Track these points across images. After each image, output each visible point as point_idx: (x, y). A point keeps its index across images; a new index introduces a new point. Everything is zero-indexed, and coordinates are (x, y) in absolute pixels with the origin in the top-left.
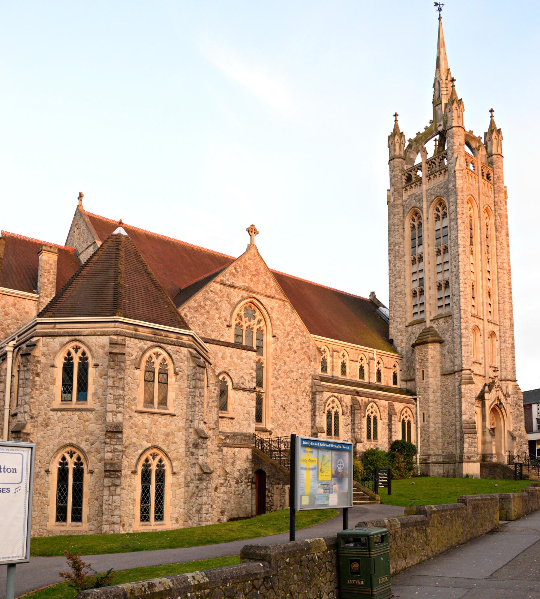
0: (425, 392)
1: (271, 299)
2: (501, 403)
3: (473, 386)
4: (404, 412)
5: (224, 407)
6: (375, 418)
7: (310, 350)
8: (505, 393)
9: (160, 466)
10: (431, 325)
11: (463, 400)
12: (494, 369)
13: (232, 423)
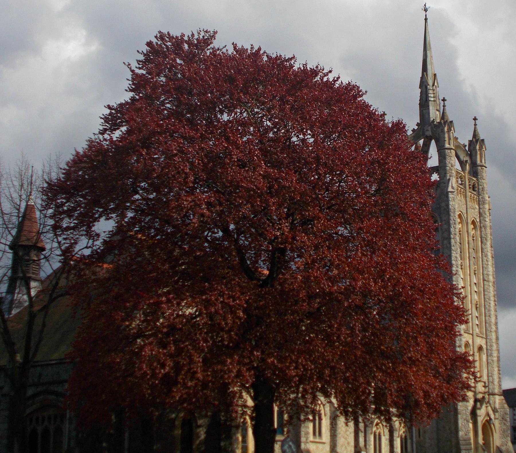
2: (490, 419)
8: (493, 407)
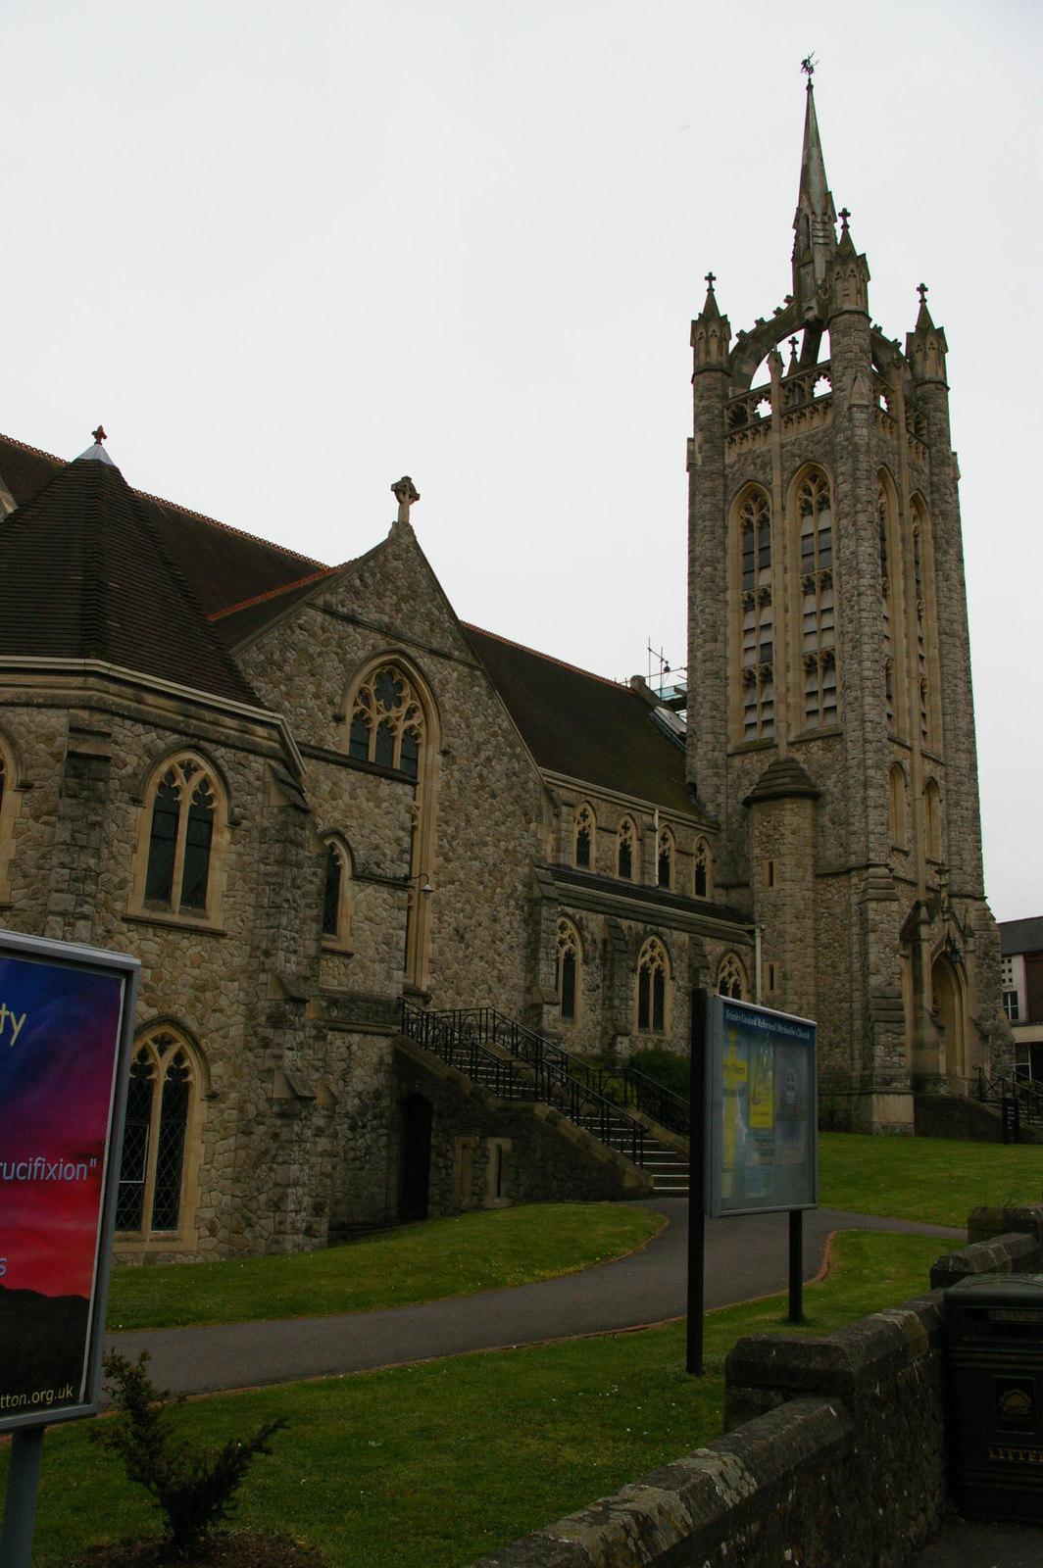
0: (776, 916)
1: (442, 660)
2: (955, 951)
3: (894, 906)
4: (725, 962)
5: (329, 923)
6: (659, 972)
7: (527, 792)
9: (178, 1073)
10: (790, 754)
11: (872, 937)
12: (937, 868)
13: (346, 966)
